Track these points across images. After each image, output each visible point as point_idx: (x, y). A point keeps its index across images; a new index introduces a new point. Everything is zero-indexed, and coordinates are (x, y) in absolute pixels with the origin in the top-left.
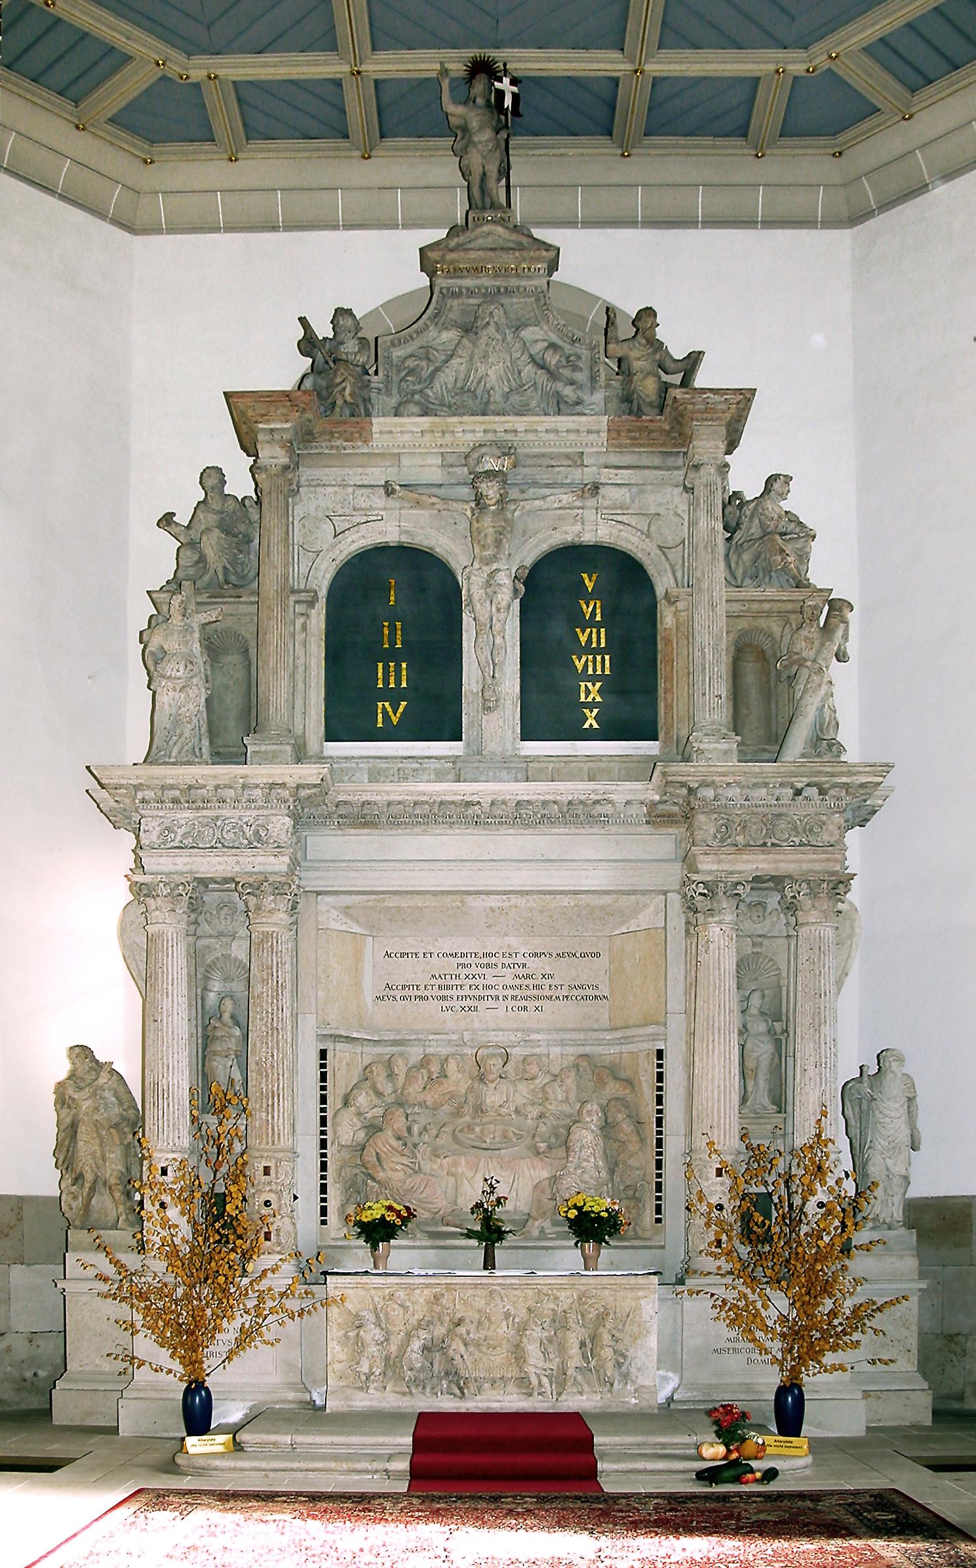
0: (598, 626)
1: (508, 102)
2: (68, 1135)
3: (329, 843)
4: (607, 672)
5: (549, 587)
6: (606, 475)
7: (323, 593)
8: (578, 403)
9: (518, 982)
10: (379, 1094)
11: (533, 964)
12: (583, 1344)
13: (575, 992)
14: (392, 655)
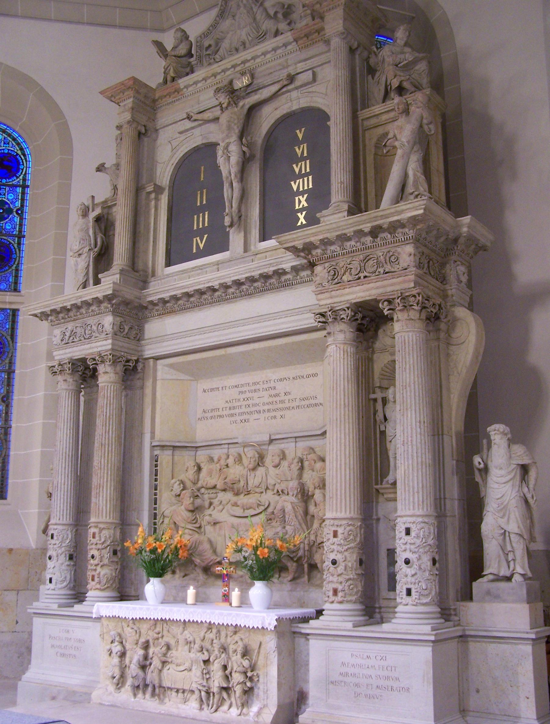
4: (311, 186)
9: (271, 400)
13: (303, 403)
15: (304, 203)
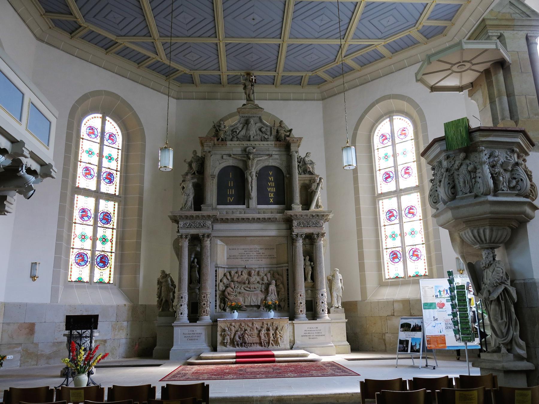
0: (273, 182)
1: (254, 81)
2: (160, 289)
3: (217, 226)
5: (262, 174)
6: (274, 152)
7: (217, 175)
8: (268, 138)
10: (228, 279)
11: (260, 251)
12: (273, 334)
14: (231, 188)
15: (272, 195)
